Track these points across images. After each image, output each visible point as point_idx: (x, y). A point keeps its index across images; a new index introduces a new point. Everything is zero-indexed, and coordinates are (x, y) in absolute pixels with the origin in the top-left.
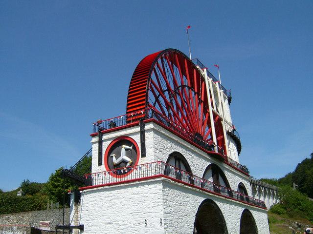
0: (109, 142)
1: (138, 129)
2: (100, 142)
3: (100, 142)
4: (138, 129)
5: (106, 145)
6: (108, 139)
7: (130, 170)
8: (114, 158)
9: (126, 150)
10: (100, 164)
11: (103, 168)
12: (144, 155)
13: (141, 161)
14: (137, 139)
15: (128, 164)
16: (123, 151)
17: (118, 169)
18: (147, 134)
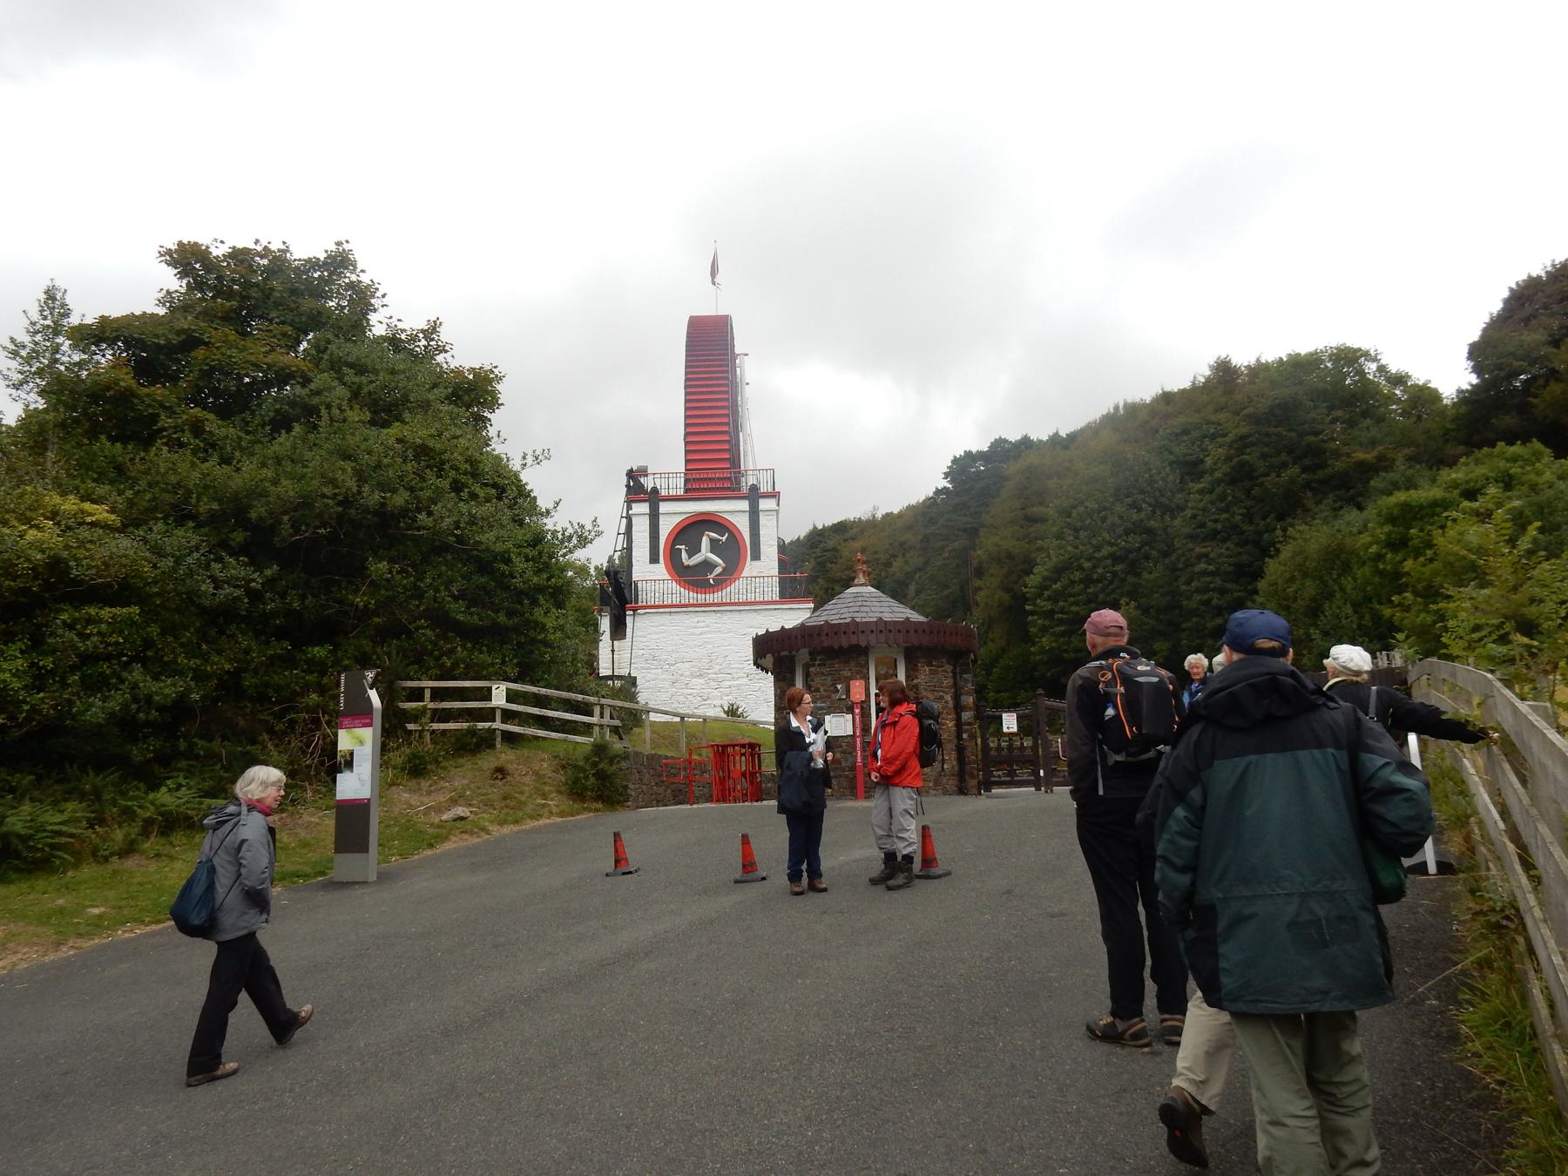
0: (678, 519)
1: (744, 505)
2: (654, 517)
3: (654, 517)
4: (744, 505)
5: (666, 527)
6: (673, 515)
7: (721, 583)
8: (684, 555)
9: (712, 541)
10: (654, 559)
11: (660, 570)
12: (756, 556)
13: (750, 568)
14: (742, 524)
15: (718, 570)
16: (705, 542)
17: (693, 577)
18: (763, 519)
